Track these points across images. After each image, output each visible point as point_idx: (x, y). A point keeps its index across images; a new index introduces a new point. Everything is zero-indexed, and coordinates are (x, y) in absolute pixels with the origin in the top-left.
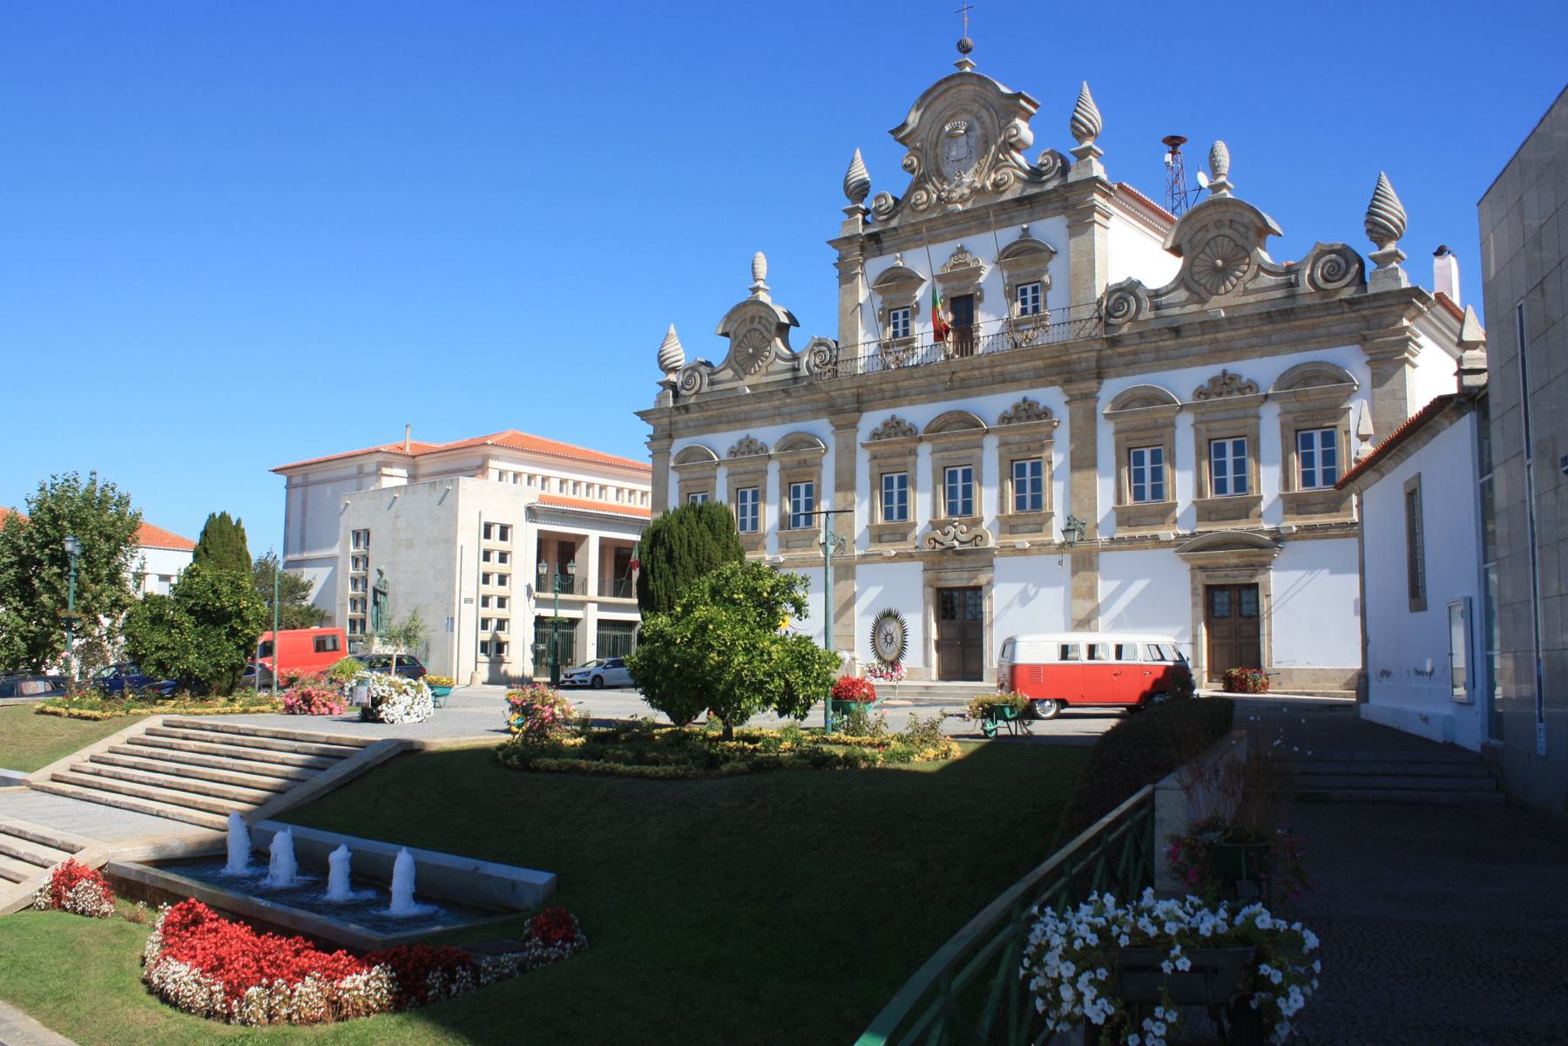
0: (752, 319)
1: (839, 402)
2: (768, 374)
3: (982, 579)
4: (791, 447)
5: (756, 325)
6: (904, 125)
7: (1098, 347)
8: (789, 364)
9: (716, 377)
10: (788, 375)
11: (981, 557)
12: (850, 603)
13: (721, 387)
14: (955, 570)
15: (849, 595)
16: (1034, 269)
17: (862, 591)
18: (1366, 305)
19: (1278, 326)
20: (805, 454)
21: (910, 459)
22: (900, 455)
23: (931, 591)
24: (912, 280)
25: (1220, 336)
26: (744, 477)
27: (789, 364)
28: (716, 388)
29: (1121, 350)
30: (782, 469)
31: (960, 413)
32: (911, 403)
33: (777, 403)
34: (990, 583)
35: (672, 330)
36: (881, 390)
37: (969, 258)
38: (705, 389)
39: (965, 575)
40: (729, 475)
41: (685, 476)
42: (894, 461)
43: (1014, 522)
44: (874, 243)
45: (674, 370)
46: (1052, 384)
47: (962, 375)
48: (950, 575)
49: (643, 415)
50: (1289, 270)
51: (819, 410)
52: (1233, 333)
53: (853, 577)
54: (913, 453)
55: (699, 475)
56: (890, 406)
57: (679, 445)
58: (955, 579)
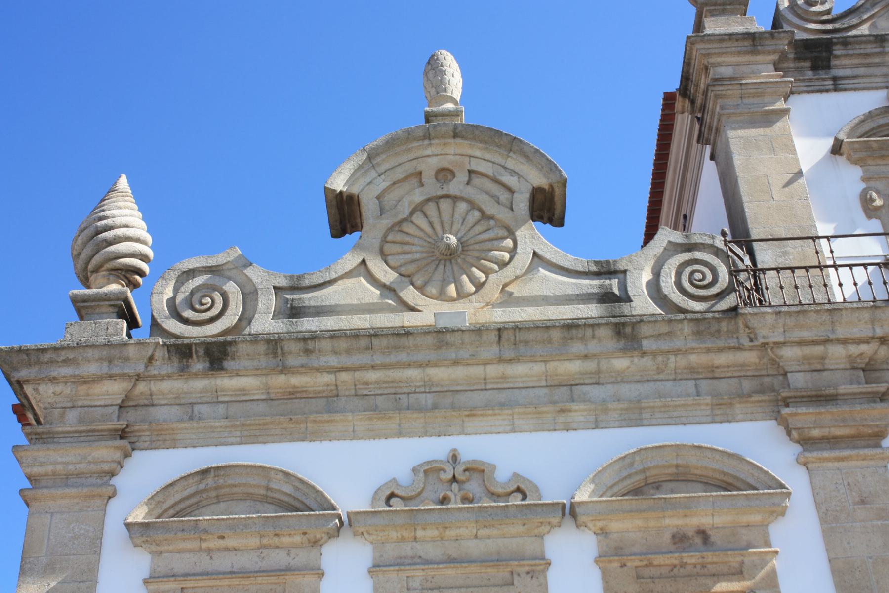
0: (444, 174)
1: (798, 380)
2: (508, 299)
4: (636, 491)
5: (456, 187)
8: (591, 285)
9: (309, 299)
10: (592, 311)
13: (329, 323)
20: (710, 513)
27: (591, 285)
28: (309, 324)
33: (575, 366)
35: (123, 183)
40: (376, 569)
41: (182, 563)
45: (129, 275)
51: (743, 396)
57: (148, 474)
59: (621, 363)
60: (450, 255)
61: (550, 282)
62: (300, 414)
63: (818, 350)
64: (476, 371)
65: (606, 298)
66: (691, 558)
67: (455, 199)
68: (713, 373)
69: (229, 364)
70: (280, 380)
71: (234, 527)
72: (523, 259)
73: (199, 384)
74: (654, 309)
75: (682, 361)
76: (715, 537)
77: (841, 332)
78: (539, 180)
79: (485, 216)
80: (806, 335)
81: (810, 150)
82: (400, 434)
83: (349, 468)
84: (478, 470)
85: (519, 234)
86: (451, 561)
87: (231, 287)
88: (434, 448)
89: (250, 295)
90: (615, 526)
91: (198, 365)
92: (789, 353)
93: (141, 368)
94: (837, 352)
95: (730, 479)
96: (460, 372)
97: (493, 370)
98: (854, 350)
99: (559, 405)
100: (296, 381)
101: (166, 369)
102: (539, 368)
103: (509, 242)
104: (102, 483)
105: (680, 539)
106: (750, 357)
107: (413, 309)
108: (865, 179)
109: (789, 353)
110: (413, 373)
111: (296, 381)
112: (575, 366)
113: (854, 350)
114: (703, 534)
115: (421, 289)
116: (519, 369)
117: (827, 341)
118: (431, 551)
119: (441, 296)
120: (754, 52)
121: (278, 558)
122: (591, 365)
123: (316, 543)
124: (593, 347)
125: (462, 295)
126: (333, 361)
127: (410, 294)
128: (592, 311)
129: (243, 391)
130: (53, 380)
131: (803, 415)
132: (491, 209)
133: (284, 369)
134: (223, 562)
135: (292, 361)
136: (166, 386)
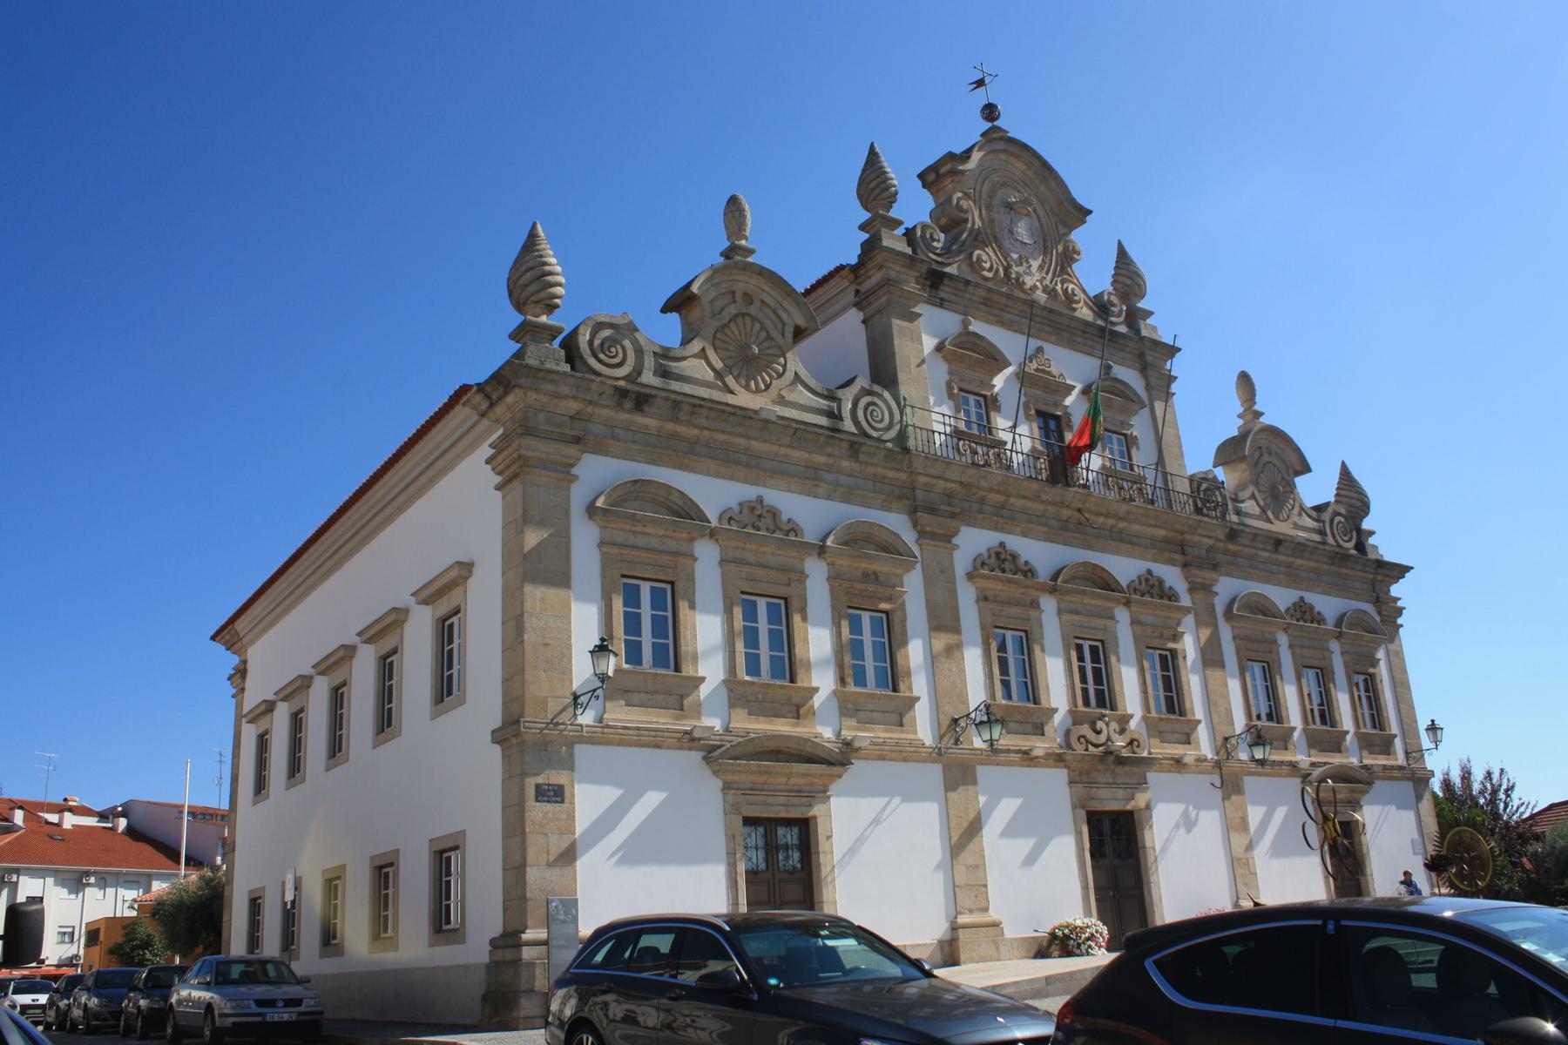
0: (748, 298)
2: (781, 401)
3: (1140, 800)
10: (823, 421)
11: (1128, 766)
12: (973, 829)
13: (687, 388)
14: (1109, 785)
15: (973, 814)
16: (1120, 417)
17: (992, 805)
20: (882, 566)
21: (1033, 614)
22: (1018, 604)
23: (1082, 814)
26: (760, 572)
27: (823, 403)
28: (675, 386)
30: (834, 578)
31: (1095, 566)
32: (1024, 534)
33: (822, 459)
34: (1148, 807)
36: (982, 500)
37: (1054, 370)
38: (648, 378)
39: (1120, 793)
42: (1015, 611)
43: (1163, 727)
46: (1172, 562)
48: (1104, 793)
53: (975, 782)
54: (1035, 605)
55: (654, 543)
56: (1002, 530)
57: (596, 473)
58: (1110, 801)
59: (845, 463)
60: (755, 358)
61: (803, 396)
62: (684, 454)
63: (934, 481)
64: (775, 449)
65: (830, 414)
66: (871, 587)
67: (754, 319)
68: (882, 480)
69: (646, 408)
70: (670, 426)
71: (654, 521)
72: (789, 376)
73: (625, 416)
74: (853, 429)
76: (881, 578)
77: (948, 475)
79: (769, 337)
80: (932, 472)
81: (929, 343)
82: (732, 478)
83: (713, 494)
84: (774, 513)
85: (789, 355)
86: (761, 566)
87: (627, 343)
88: (748, 492)
89: (639, 352)
90: (840, 562)
91: (628, 404)
93: (596, 398)
94: (942, 484)
95: (890, 546)
96: (766, 447)
97: (783, 450)
99: (810, 480)
100: (680, 429)
102: (806, 455)
103: (782, 360)
104: (565, 473)
105: (865, 575)
106: (903, 476)
107: (732, 392)
108: (950, 373)
109: (922, 479)
110: (743, 441)
111: (680, 429)
112: (822, 459)
113: (949, 485)
114: (875, 574)
115: (736, 379)
118: (751, 558)
119: (747, 387)
120: (909, 268)
121: (672, 545)
122: (830, 461)
123: (692, 540)
125: (758, 391)
126: (705, 423)
127: (730, 380)
128: (823, 421)
129: (647, 427)
130: (538, 390)
131: (924, 518)
132: (774, 334)
133: (676, 420)
134: (641, 541)
135: (682, 416)
136: (605, 412)
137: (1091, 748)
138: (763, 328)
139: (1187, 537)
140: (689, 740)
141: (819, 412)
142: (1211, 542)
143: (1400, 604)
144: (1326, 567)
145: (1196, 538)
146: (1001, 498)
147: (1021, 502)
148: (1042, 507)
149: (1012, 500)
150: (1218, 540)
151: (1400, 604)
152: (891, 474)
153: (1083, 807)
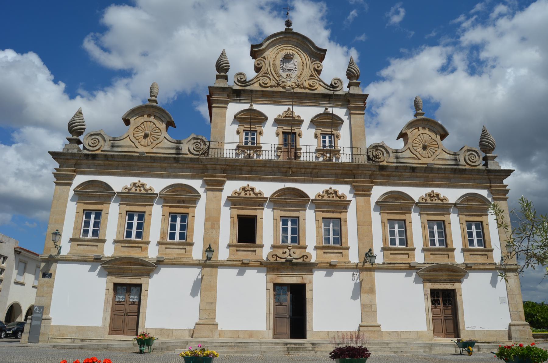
6: (261, 45)
7: (374, 169)
10: (174, 151)
18: (494, 174)
19: (456, 175)
24: (262, 119)
25: (431, 175)
29: (383, 173)
31: (294, 189)
44: (237, 95)
47: (294, 170)
49: (55, 155)
50: (455, 154)
52: (437, 175)
57: (79, 180)
59: (175, 165)
64: (146, 164)
70: (107, 162)
73: (91, 162)
75: (187, 166)
78: (168, 120)
92: (208, 166)
93: (78, 158)
94: (218, 166)
95: (191, 190)
96: (143, 164)
97: (149, 164)
98: (222, 166)
101: (84, 158)
102: (159, 164)
107: (137, 148)
109: (208, 166)
111: (110, 163)
112: (166, 165)
113: (222, 166)
116: (155, 164)
117: (216, 165)
122: (169, 165)
124: (170, 162)
129: (100, 164)
130: (61, 159)
136: (84, 161)
137: (278, 259)
138: (154, 124)
139: (354, 171)
140: (97, 260)
141: (172, 148)
142: (370, 172)
143: (507, 188)
144: (451, 175)
145: (360, 172)
146: (249, 168)
147: (259, 168)
148: (270, 169)
149: (254, 168)
150: (374, 171)
151: (507, 188)
152: (196, 166)
153: (272, 282)
